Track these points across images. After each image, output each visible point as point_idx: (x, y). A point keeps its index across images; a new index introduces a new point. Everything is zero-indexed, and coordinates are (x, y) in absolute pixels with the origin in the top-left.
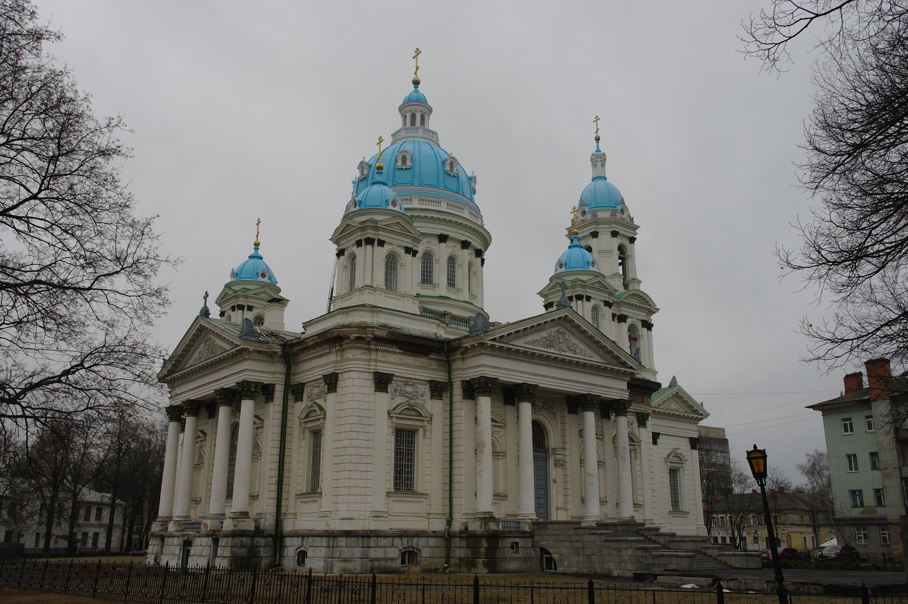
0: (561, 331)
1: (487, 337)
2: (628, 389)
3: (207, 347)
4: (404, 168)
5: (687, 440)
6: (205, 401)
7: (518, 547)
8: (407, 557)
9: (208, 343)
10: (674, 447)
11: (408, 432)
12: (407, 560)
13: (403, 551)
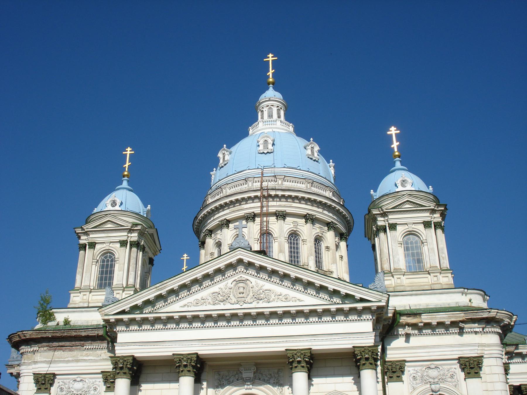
4: (314, 159)
9: (241, 285)
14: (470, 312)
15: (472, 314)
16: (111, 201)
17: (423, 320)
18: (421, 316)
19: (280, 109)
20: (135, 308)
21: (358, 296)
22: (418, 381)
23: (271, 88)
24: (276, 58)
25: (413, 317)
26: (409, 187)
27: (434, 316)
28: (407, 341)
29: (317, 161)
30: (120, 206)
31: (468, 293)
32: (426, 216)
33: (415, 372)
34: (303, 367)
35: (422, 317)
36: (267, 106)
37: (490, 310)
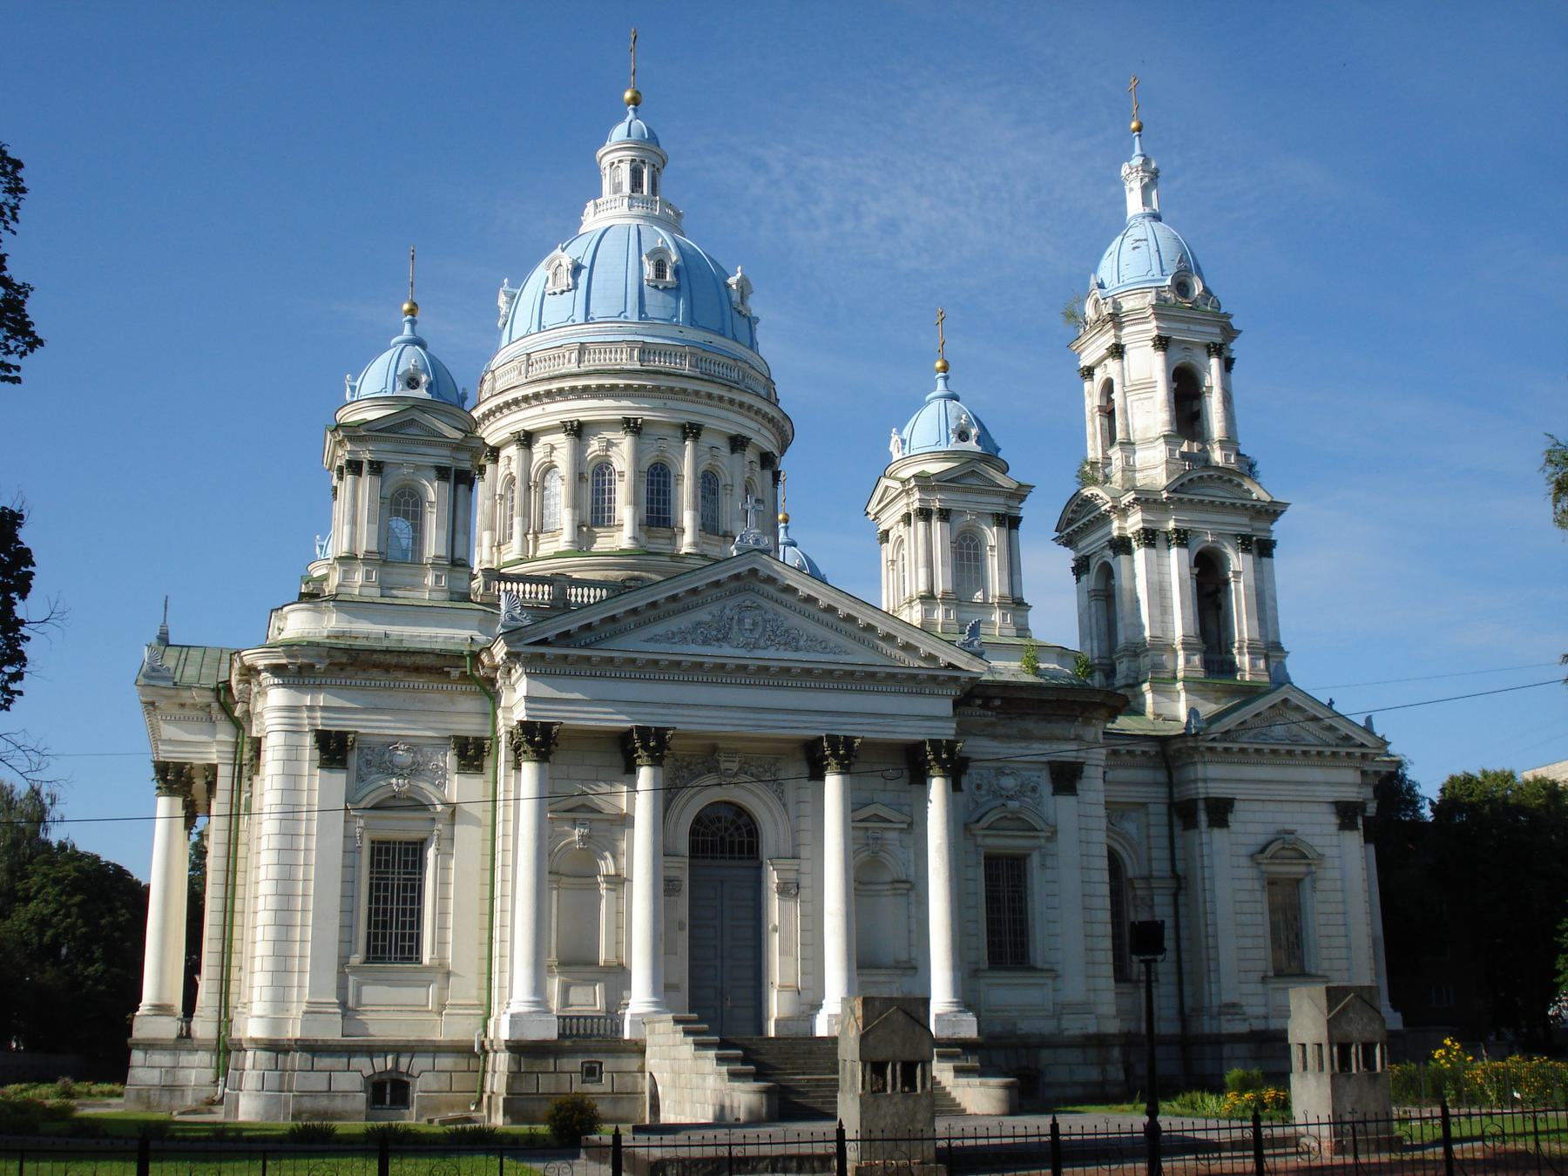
0: (748, 603)
1: (519, 640)
2: (955, 715)
4: (558, 291)
5: (1333, 809)
7: (601, 1073)
8: (388, 1091)
10: (1280, 827)
11: (406, 843)
12: (388, 1097)
13: (376, 1078)
19: (621, 165)
29: (570, 290)
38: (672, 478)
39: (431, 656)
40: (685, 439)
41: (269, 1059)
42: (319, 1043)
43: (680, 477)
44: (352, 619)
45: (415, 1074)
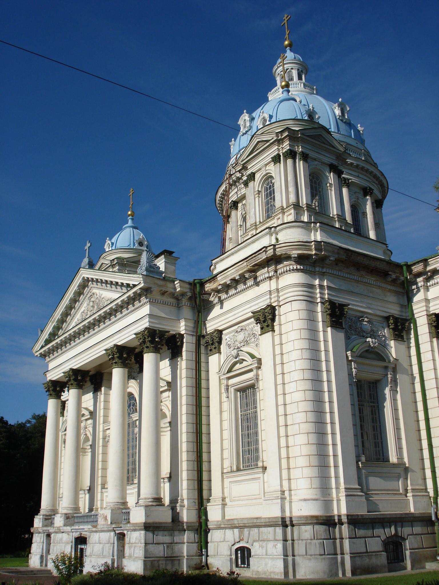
3: (91, 304)
6: (88, 372)
9: (92, 300)
14: (249, 258)
15: (252, 259)
16: (107, 245)
17: (222, 281)
18: (217, 278)
20: (47, 342)
21: (131, 283)
22: (232, 349)
23: (288, 51)
24: (289, 16)
25: (213, 282)
26: (268, 123)
27: (226, 275)
28: (221, 308)
30: (112, 247)
31: (279, 231)
32: (273, 151)
33: (229, 340)
34: (116, 363)
35: (218, 279)
36: (279, 74)
37: (264, 249)
38: (360, 215)
39: (384, 263)
40: (365, 195)
41: (325, 530)
42: (360, 517)
43: (365, 214)
44: (329, 238)
45: (406, 538)
